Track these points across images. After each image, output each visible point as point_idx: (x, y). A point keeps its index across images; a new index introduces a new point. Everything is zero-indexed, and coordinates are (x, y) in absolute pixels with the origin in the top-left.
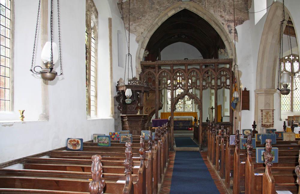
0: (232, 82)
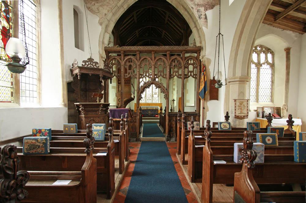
0: (199, 71)
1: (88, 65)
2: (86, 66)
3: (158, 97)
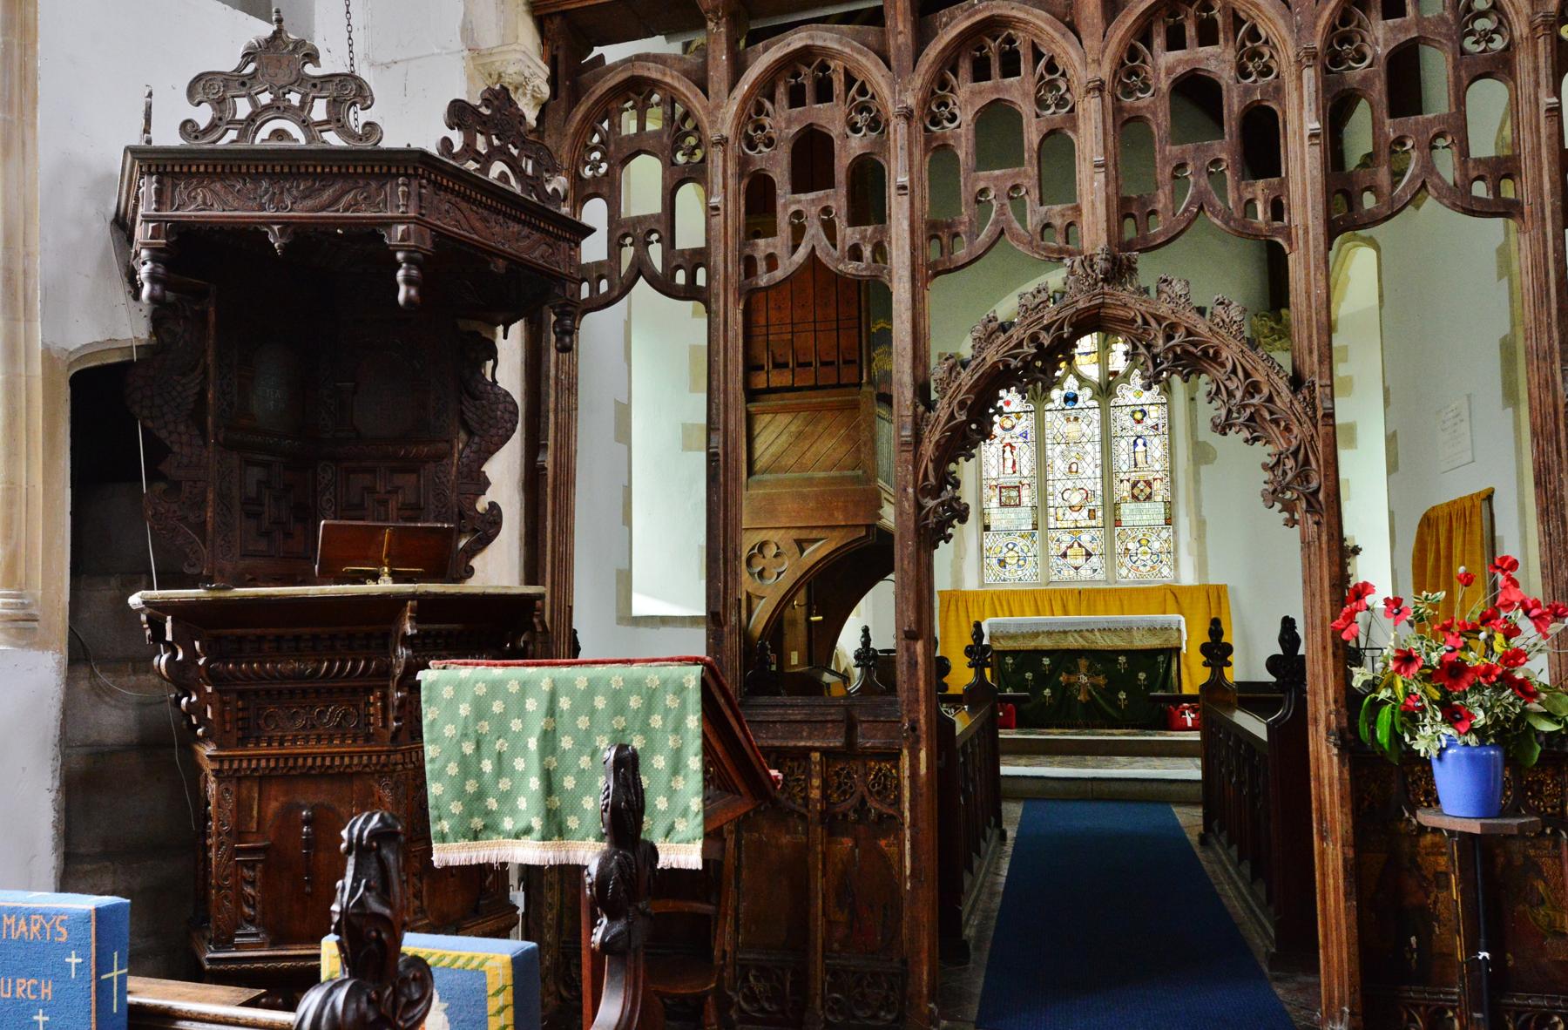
1: (251, 119)
2: (232, 135)
3: (1168, 521)
